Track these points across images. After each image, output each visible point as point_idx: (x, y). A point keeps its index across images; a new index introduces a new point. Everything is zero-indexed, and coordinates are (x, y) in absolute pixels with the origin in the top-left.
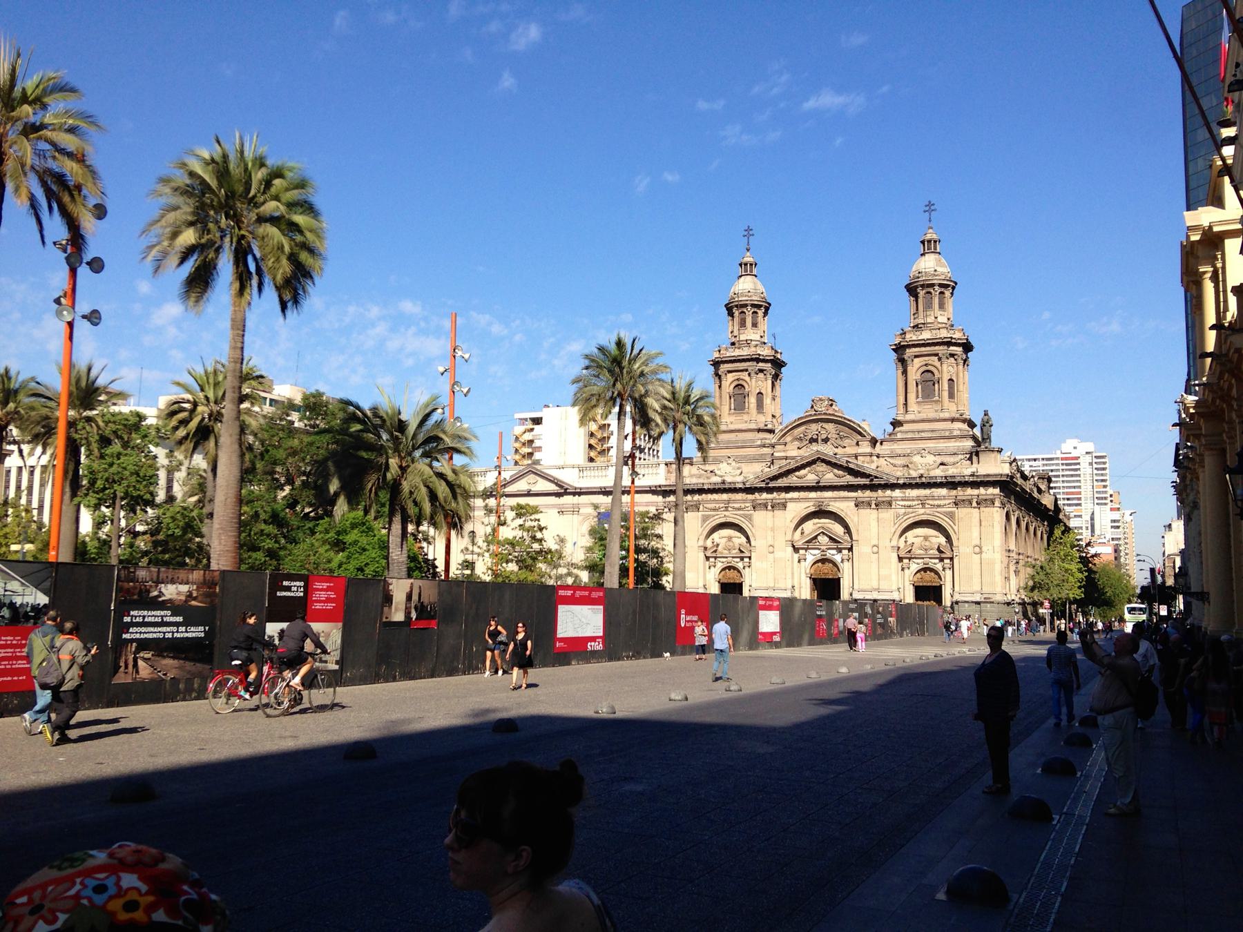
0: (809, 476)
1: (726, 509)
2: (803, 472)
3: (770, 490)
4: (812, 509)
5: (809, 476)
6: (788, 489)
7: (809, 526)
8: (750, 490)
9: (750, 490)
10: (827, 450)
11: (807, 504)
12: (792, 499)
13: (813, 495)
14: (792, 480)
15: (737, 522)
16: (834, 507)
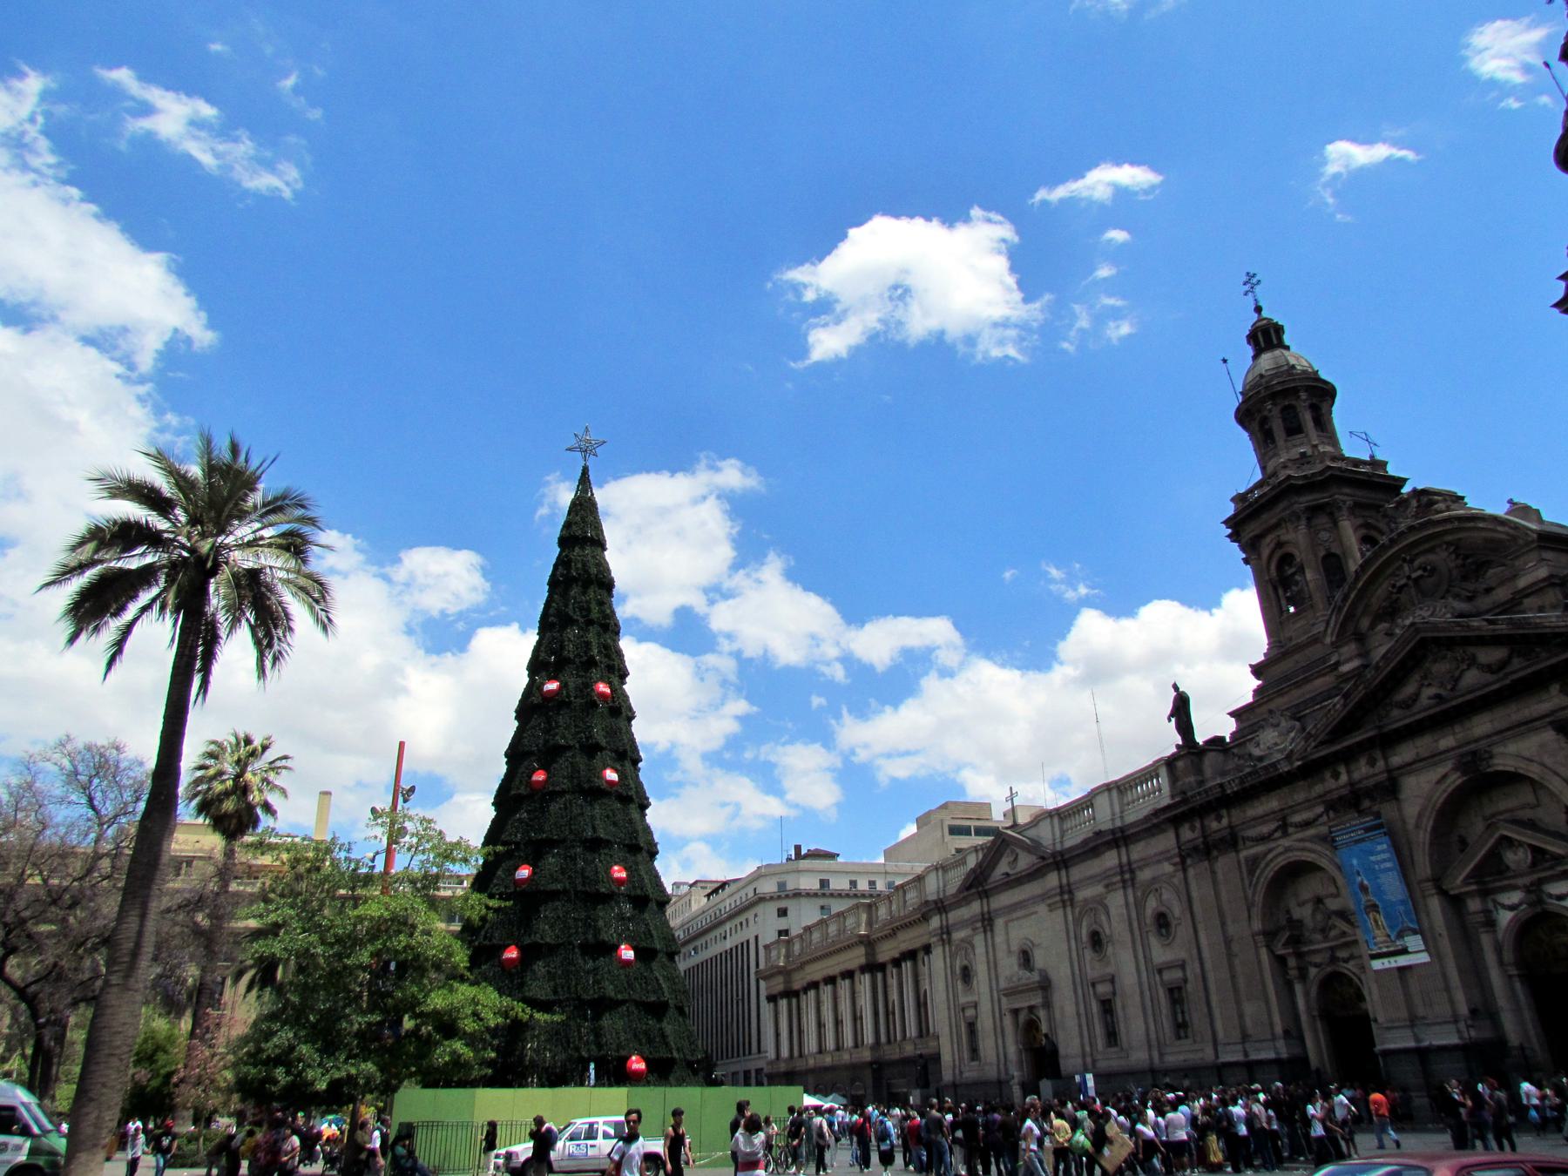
0: (1423, 693)
1: (1284, 828)
2: (1409, 689)
3: (1348, 757)
4: (1456, 780)
5: (1423, 693)
6: (1388, 741)
7: (1474, 827)
8: (1310, 770)
9: (1310, 770)
10: (1435, 614)
11: (1441, 770)
12: (1408, 768)
13: (1447, 742)
14: (1397, 718)
15: (1309, 857)
16: (1506, 758)
